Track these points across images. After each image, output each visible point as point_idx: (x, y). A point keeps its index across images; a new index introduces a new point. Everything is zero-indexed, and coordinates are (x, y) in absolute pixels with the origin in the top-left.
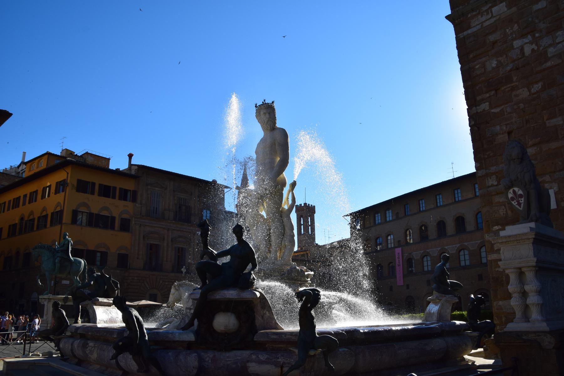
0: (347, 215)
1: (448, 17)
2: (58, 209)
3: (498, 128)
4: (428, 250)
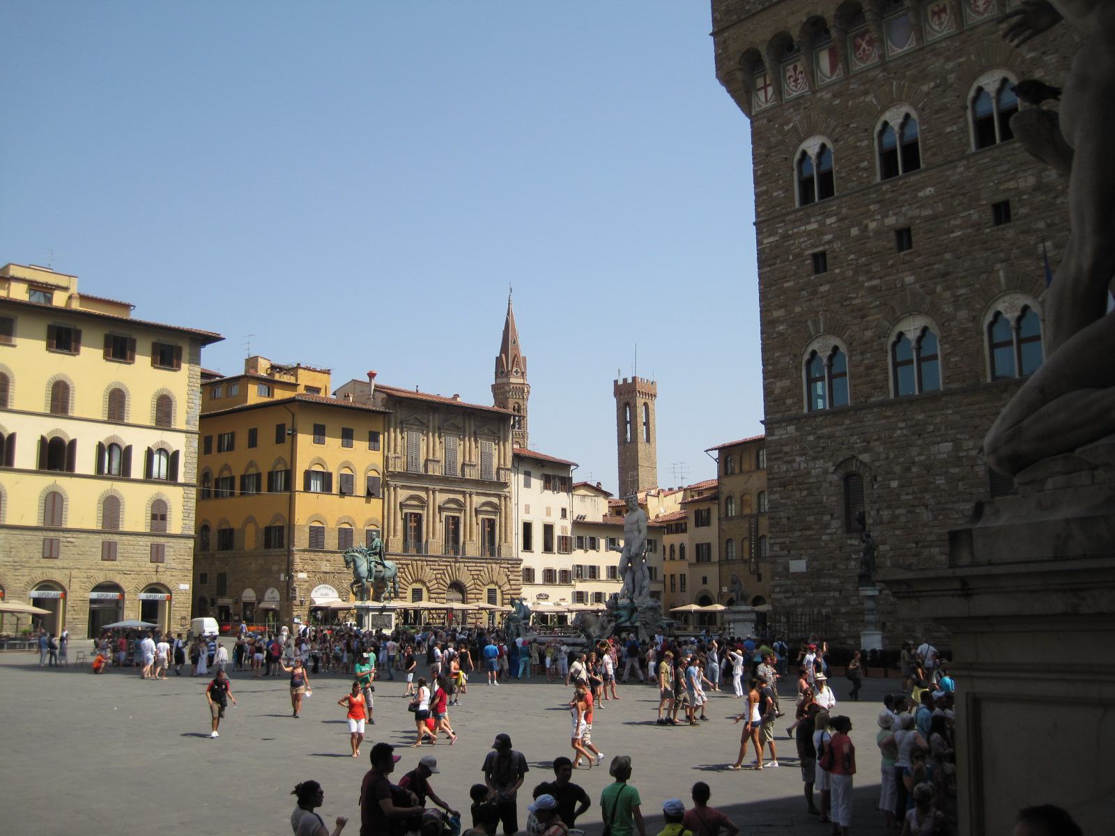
0: (712, 450)
1: (762, 422)
2: (281, 467)
3: (782, 514)
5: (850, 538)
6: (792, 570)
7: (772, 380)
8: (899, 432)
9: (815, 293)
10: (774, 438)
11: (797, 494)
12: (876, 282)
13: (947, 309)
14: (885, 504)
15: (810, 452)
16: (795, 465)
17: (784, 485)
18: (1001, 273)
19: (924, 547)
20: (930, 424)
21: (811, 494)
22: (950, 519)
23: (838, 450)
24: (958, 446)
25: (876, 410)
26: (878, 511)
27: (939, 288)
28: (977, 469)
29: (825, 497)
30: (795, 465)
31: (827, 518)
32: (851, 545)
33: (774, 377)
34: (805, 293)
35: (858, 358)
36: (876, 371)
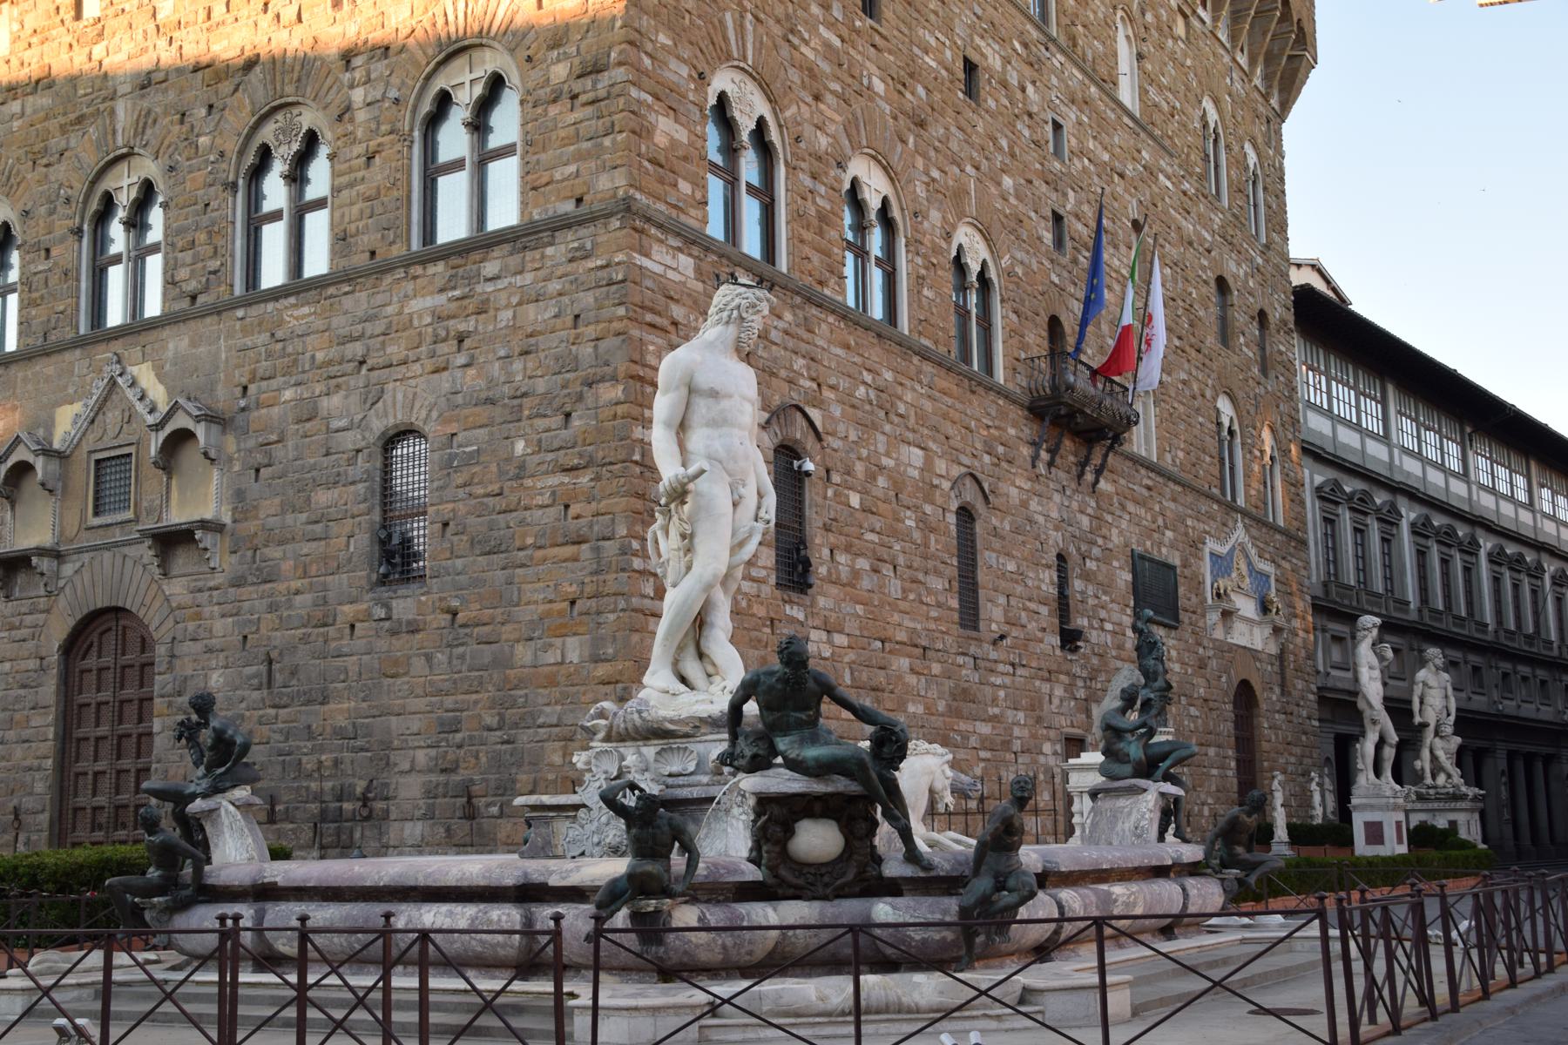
5: (791, 602)
7: (650, 99)
8: (861, 391)
10: (646, 262)
14: (843, 538)
19: (890, 652)
20: (900, 399)
22: (922, 602)
23: (773, 374)
24: (928, 467)
25: (831, 319)
26: (832, 551)
28: (947, 515)
32: (793, 620)
35: (808, 182)
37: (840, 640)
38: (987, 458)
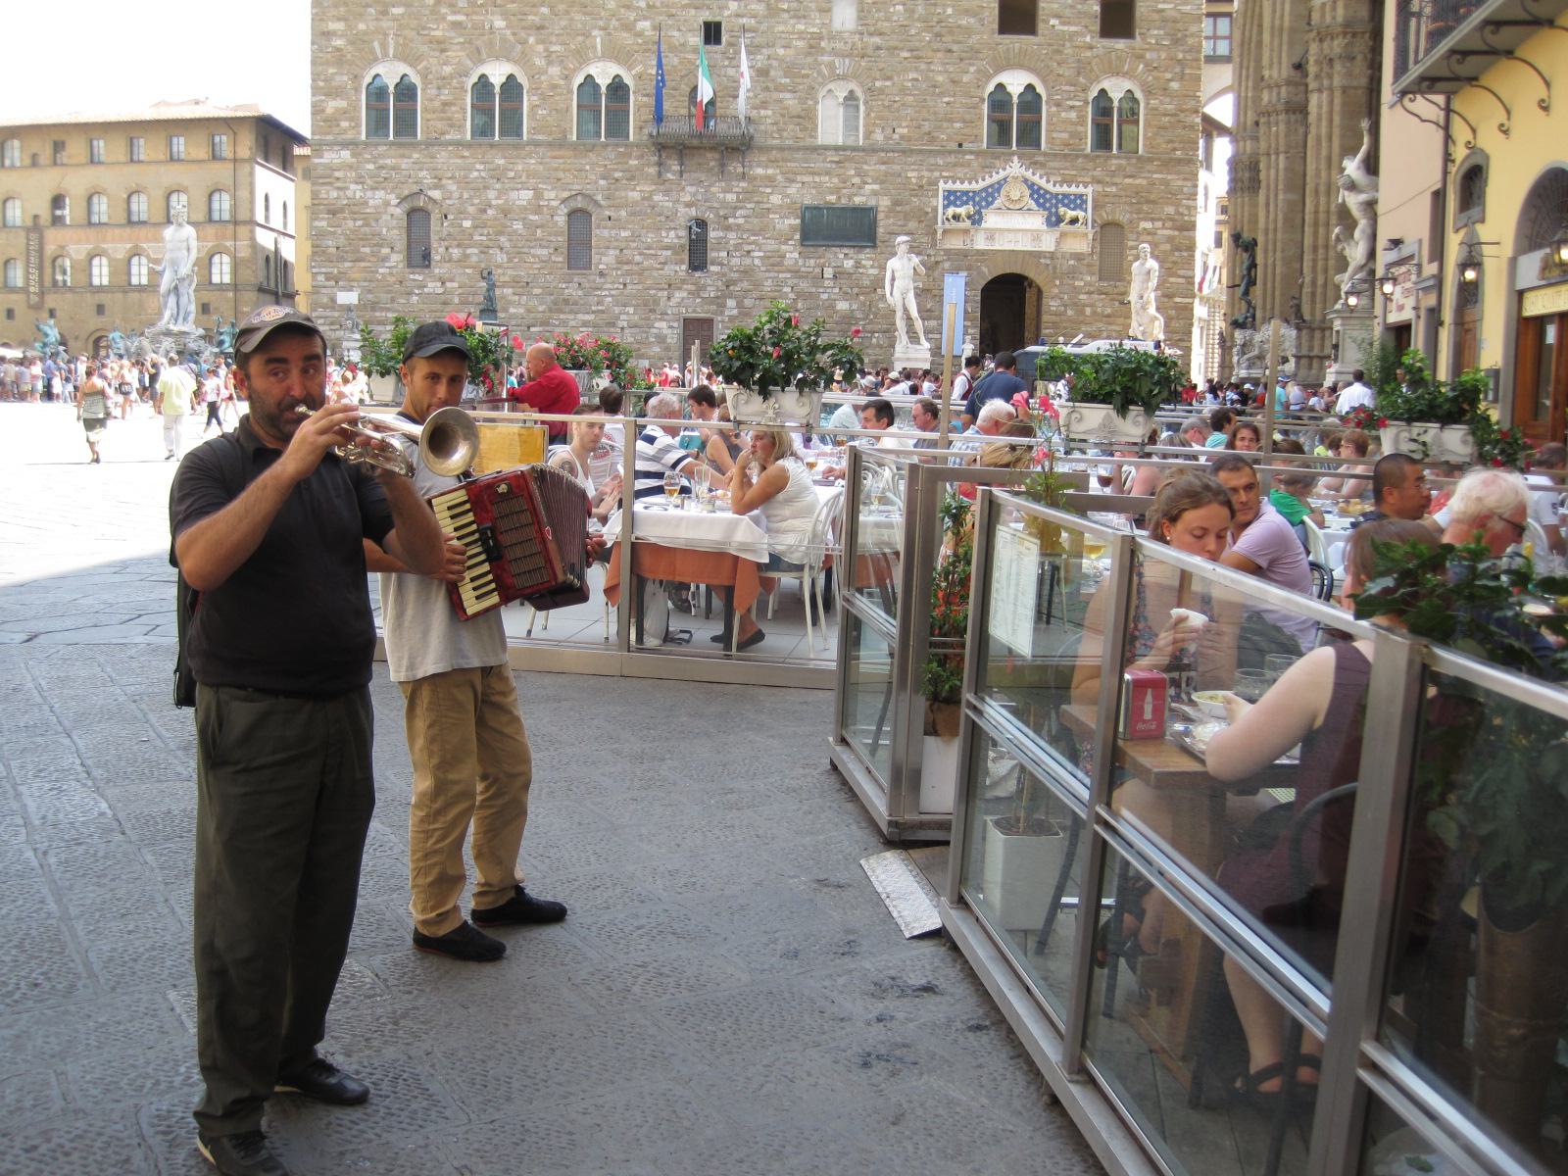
4: (105, 246)
6: (340, 301)
8: (476, 174)
9: (385, 13)
11: (350, 223)
12: (460, 18)
13: (539, 62)
15: (369, 181)
16: (349, 193)
17: (333, 213)
18: (598, 40)
21: (367, 225)
24: (538, 195)
27: (532, 40)
28: (556, 218)
29: (384, 231)
30: (349, 193)
31: (385, 251)
33: (326, 95)
34: (372, 10)
35: (434, 92)
36: (453, 109)
37: (448, 284)
38: (602, 182)
